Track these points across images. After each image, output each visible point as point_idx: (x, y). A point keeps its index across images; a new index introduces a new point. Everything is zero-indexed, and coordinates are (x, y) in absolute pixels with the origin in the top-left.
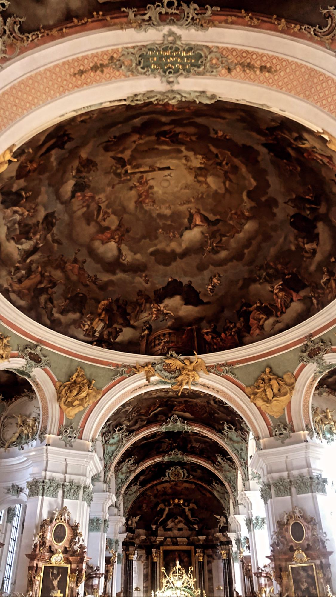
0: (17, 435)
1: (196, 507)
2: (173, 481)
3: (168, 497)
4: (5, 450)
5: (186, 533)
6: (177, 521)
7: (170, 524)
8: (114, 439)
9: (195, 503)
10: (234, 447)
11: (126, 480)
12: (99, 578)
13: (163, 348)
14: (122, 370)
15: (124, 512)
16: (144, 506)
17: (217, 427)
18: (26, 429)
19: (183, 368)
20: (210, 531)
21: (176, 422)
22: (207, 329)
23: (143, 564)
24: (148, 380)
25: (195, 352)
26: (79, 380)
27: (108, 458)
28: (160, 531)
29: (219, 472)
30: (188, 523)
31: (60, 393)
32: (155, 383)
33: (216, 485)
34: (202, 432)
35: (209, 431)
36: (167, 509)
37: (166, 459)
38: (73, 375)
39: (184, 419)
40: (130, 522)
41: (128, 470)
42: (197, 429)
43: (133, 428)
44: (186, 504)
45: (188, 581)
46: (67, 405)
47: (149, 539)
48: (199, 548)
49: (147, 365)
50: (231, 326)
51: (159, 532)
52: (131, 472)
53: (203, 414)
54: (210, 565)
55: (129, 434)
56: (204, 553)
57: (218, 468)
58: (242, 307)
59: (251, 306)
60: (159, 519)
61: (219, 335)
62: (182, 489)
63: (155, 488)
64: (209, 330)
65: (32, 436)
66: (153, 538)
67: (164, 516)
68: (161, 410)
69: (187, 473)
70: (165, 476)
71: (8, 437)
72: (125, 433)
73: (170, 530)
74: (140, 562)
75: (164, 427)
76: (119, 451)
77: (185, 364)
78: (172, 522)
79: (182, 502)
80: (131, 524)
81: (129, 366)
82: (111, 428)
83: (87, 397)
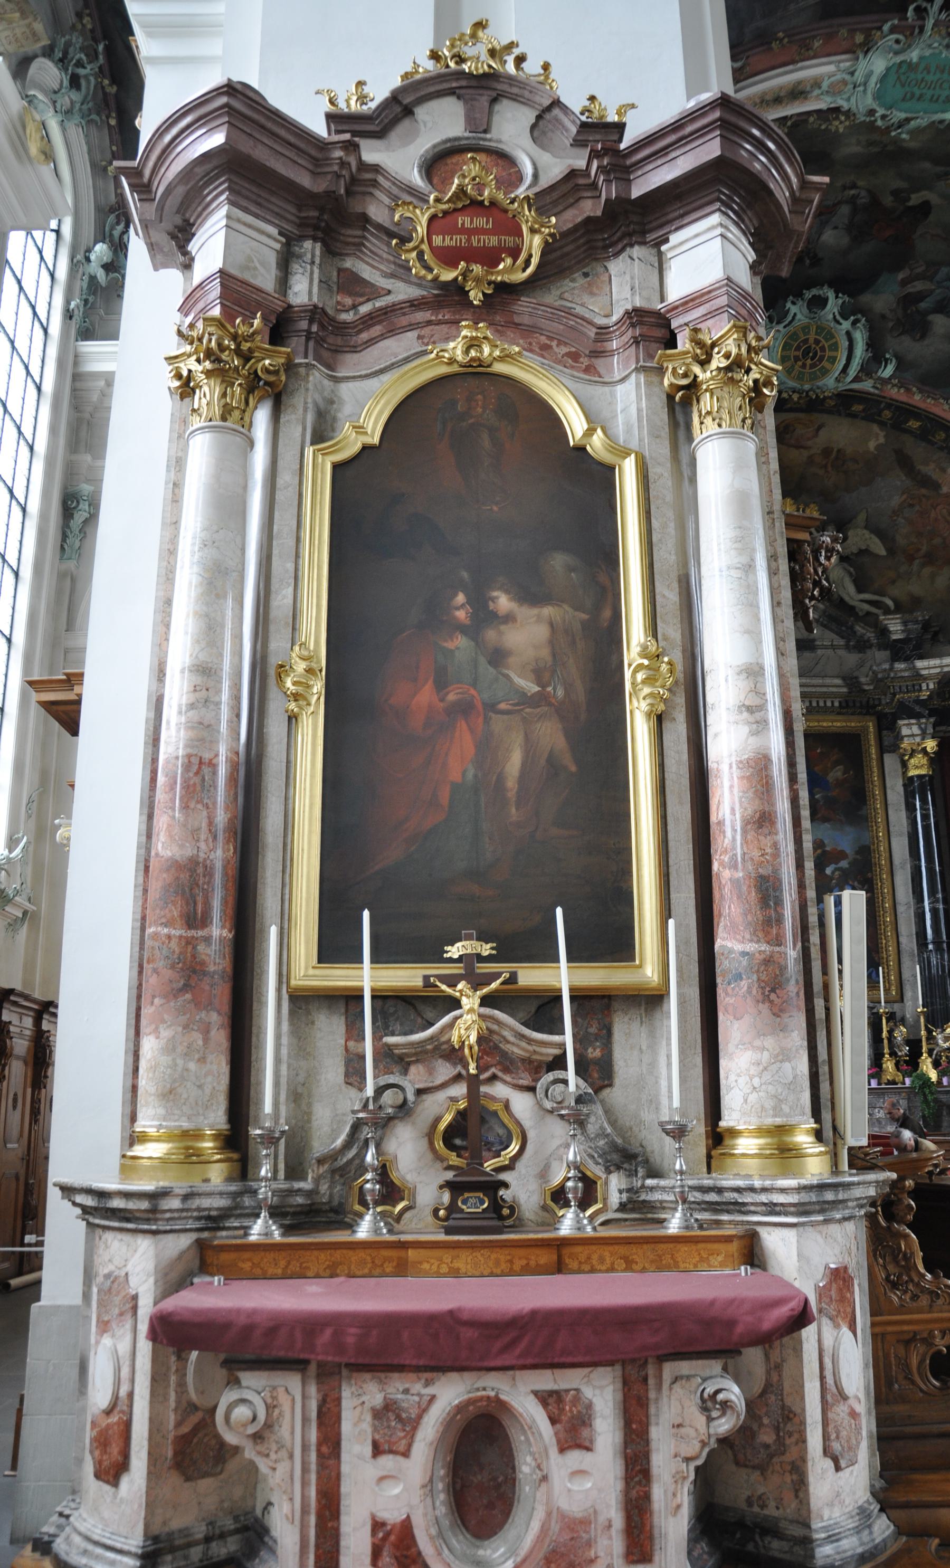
1: (879, 549)
62: (811, 460)
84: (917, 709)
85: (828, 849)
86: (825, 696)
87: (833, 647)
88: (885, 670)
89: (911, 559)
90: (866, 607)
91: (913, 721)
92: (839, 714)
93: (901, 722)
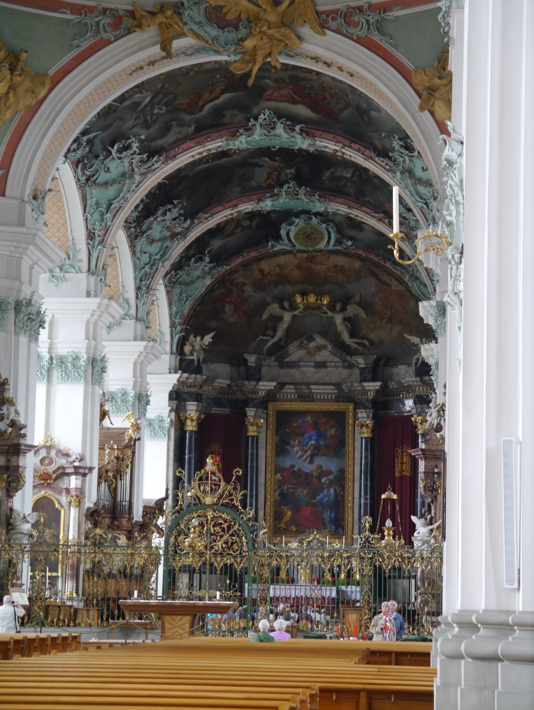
1: (362, 314)
3: (289, 289)
6: (312, 345)
9: (359, 304)
10: (418, 194)
11: (162, 256)
12: (84, 475)
14: (98, 23)
15: (173, 325)
16: (228, 309)
17: (377, 143)
19: (258, 19)
20: (395, 370)
21: (274, 128)
24: (166, 47)
27: (97, 216)
32: (189, 52)
34: (343, 153)
35: (359, 150)
36: (287, 317)
37: (267, 205)
40: (187, 349)
41: (168, 234)
44: (338, 306)
45: (231, 495)
47: (237, 386)
48: (365, 408)
51: (264, 370)
52: (174, 236)
53: (342, 110)
55: (151, 156)
60: (267, 341)
62: (328, 270)
63: (255, 267)
66: (249, 385)
67: (280, 333)
69: (339, 231)
70: (278, 238)
72: (137, 158)
73: (292, 365)
75: (243, 139)
76: (126, 200)
78: (301, 346)
80: (192, 354)
82: (98, 145)
83: (11, 95)
84: (367, 404)
85: (324, 469)
86: (328, 394)
87: (336, 367)
88: (349, 386)
89: (382, 318)
91: (363, 410)
92: (336, 401)
93: (358, 411)
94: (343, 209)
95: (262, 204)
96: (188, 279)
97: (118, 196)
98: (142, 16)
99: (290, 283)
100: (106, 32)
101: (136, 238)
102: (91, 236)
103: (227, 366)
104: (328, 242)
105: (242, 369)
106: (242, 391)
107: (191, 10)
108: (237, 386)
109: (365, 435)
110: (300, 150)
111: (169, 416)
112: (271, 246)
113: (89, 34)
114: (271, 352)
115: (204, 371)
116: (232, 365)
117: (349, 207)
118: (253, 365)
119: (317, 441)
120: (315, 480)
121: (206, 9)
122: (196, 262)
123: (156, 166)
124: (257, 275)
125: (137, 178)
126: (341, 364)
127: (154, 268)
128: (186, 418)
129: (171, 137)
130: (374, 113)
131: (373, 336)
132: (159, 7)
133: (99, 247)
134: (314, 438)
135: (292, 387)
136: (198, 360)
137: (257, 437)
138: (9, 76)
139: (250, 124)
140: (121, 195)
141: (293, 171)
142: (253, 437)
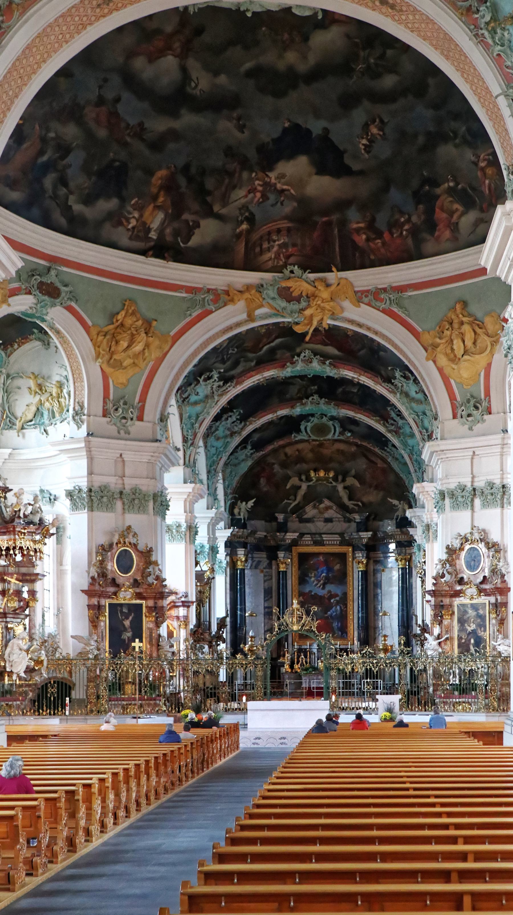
0: (33, 409)
2: (313, 440)
3: (305, 466)
4: (18, 432)
5: (339, 526)
6: (322, 506)
7: (310, 511)
8: (197, 394)
9: (354, 477)
13: (277, 256)
14: (204, 299)
15: (226, 494)
16: (263, 481)
17: (383, 372)
18: (48, 400)
21: (311, 362)
22: (358, 223)
23: (262, 575)
25: (334, 269)
26: (129, 321)
28: (294, 523)
29: (393, 436)
30: (343, 507)
31: (99, 347)
33: (393, 449)
34: (359, 379)
37: (298, 411)
38: (118, 313)
39: (324, 357)
40: (236, 511)
41: (228, 433)
42: (349, 374)
43: (233, 372)
44: (340, 478)
46: (114, 367)
48: (361, 550)
49: (248, 288)
50: (402, 220)
51: (289, 524)
53: (359, 350)
54: (379, 575)
56: (368, 558)
57: (393, 428)
58: (422, 185)
59: (438, 185)
61: (379, 234)
64: (362, 225)
65: (61, 413)
67: (299, 498)
68: (281, 343)
69: (342, 426)
70: (299, 431)
71: (19, 413)
74: (258, 571)
75: (289, 370)
76: (208, 413)
77: (315, 287)
78: (314, 507)
79: (331, 475)
81: (216, 290)
82: (192, 377)
83: (146, 351)
84: (362, 547)
86: (334, 540)
87: (339, 521)
90: (352, 506)
92: (340, 545)
94: (351, 414)
95: (293, 410)
96: (236, 461)
97: (203, 411)
98: (235, 294)
99: (306, 462)
100: (209, 305)
101: (208, 436)
102: (185, 440)
103: (263, 522)
104: (334, 434)
105: (274, 524)
106: (274, 539)
107: (269, 290)
108: (271, 536)
109: (361, 569)
110: (328, 377)
111: (225, 559)
112: (295, 437)
113: (198, 307)
114: (293, 511)
115: (248, 527)
116: (266, 521)
117: (356, 412)
118: (282, 521)
119: (327, 573)
120: (327, 601)
121: (278, 288)
122: (242, 449)
123: (229, 389)
124: (282, 457)
125: (216, 398)
126: (343, 519)
127: (219, 457)
128: (237, 560)
129: (240, 369)
130: (382, 353)
131: (365, 499)
132: (245, 287)
133: (191, 448)
134: (325, 571)
135: (309, 536)
136: (244, 519)
137: (286, 572)
138: (145, 338)
139: (294, 359)
140: (205, 410)
141: (316, 387)
142: (283, 572)
